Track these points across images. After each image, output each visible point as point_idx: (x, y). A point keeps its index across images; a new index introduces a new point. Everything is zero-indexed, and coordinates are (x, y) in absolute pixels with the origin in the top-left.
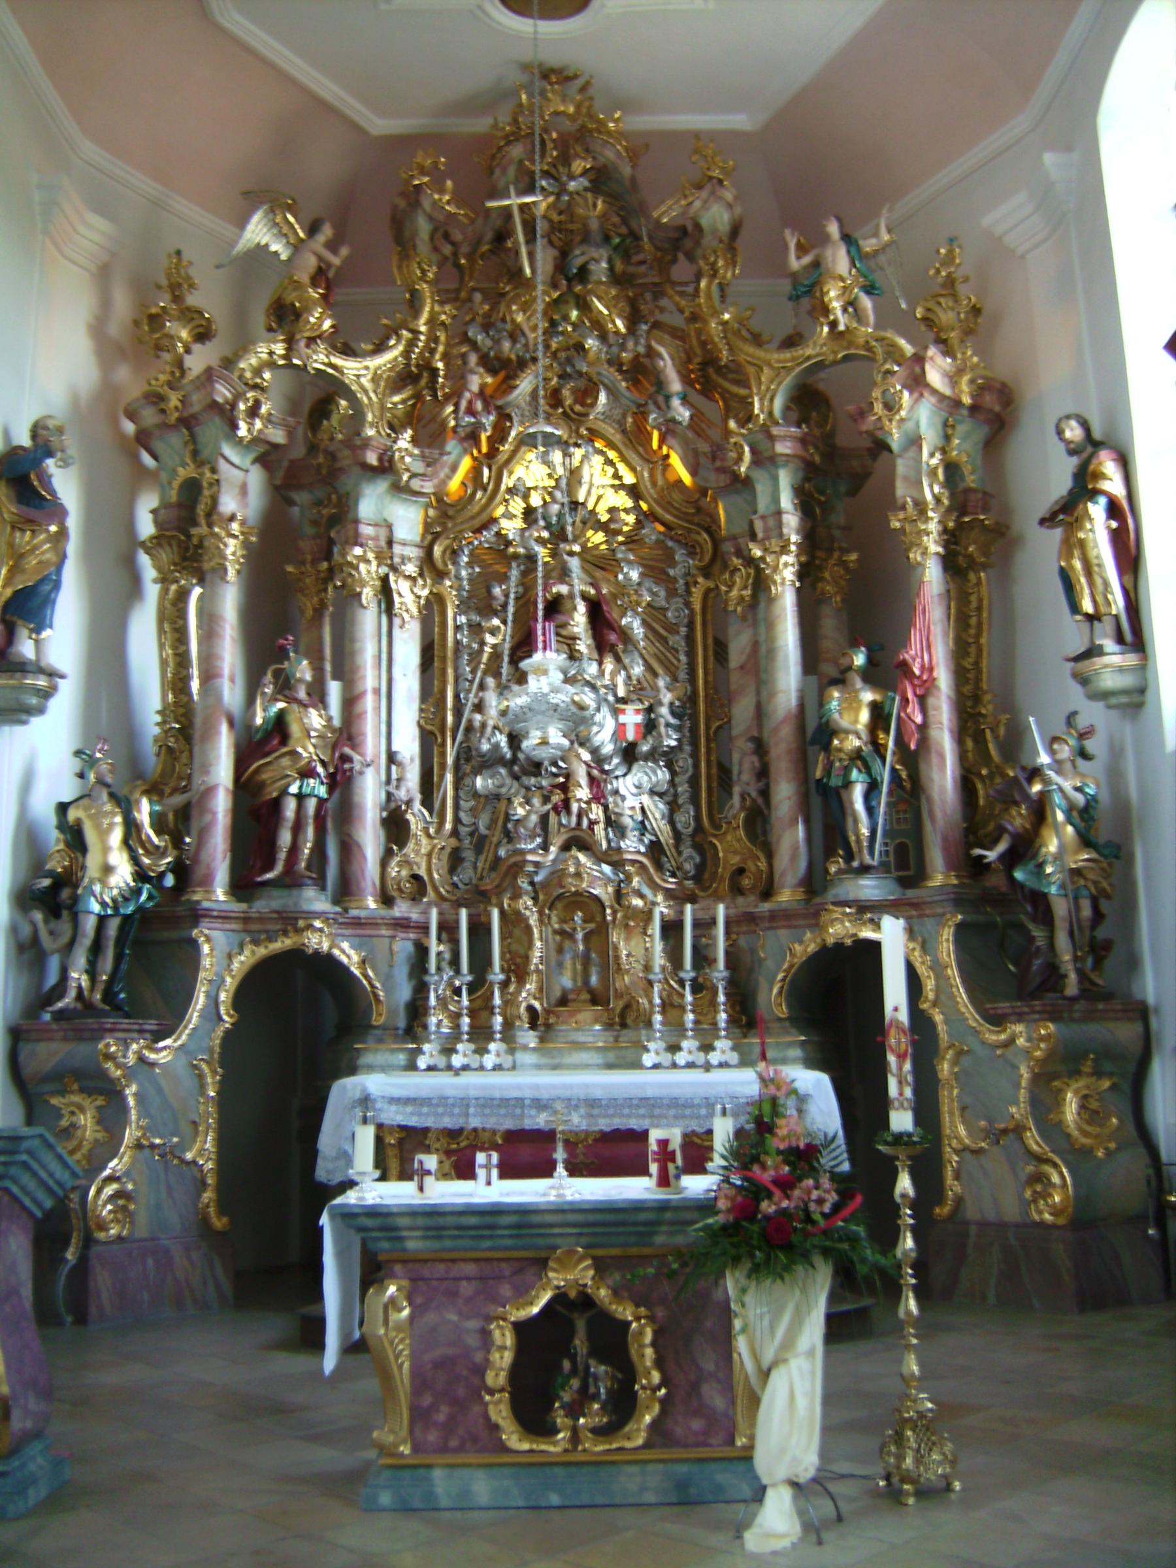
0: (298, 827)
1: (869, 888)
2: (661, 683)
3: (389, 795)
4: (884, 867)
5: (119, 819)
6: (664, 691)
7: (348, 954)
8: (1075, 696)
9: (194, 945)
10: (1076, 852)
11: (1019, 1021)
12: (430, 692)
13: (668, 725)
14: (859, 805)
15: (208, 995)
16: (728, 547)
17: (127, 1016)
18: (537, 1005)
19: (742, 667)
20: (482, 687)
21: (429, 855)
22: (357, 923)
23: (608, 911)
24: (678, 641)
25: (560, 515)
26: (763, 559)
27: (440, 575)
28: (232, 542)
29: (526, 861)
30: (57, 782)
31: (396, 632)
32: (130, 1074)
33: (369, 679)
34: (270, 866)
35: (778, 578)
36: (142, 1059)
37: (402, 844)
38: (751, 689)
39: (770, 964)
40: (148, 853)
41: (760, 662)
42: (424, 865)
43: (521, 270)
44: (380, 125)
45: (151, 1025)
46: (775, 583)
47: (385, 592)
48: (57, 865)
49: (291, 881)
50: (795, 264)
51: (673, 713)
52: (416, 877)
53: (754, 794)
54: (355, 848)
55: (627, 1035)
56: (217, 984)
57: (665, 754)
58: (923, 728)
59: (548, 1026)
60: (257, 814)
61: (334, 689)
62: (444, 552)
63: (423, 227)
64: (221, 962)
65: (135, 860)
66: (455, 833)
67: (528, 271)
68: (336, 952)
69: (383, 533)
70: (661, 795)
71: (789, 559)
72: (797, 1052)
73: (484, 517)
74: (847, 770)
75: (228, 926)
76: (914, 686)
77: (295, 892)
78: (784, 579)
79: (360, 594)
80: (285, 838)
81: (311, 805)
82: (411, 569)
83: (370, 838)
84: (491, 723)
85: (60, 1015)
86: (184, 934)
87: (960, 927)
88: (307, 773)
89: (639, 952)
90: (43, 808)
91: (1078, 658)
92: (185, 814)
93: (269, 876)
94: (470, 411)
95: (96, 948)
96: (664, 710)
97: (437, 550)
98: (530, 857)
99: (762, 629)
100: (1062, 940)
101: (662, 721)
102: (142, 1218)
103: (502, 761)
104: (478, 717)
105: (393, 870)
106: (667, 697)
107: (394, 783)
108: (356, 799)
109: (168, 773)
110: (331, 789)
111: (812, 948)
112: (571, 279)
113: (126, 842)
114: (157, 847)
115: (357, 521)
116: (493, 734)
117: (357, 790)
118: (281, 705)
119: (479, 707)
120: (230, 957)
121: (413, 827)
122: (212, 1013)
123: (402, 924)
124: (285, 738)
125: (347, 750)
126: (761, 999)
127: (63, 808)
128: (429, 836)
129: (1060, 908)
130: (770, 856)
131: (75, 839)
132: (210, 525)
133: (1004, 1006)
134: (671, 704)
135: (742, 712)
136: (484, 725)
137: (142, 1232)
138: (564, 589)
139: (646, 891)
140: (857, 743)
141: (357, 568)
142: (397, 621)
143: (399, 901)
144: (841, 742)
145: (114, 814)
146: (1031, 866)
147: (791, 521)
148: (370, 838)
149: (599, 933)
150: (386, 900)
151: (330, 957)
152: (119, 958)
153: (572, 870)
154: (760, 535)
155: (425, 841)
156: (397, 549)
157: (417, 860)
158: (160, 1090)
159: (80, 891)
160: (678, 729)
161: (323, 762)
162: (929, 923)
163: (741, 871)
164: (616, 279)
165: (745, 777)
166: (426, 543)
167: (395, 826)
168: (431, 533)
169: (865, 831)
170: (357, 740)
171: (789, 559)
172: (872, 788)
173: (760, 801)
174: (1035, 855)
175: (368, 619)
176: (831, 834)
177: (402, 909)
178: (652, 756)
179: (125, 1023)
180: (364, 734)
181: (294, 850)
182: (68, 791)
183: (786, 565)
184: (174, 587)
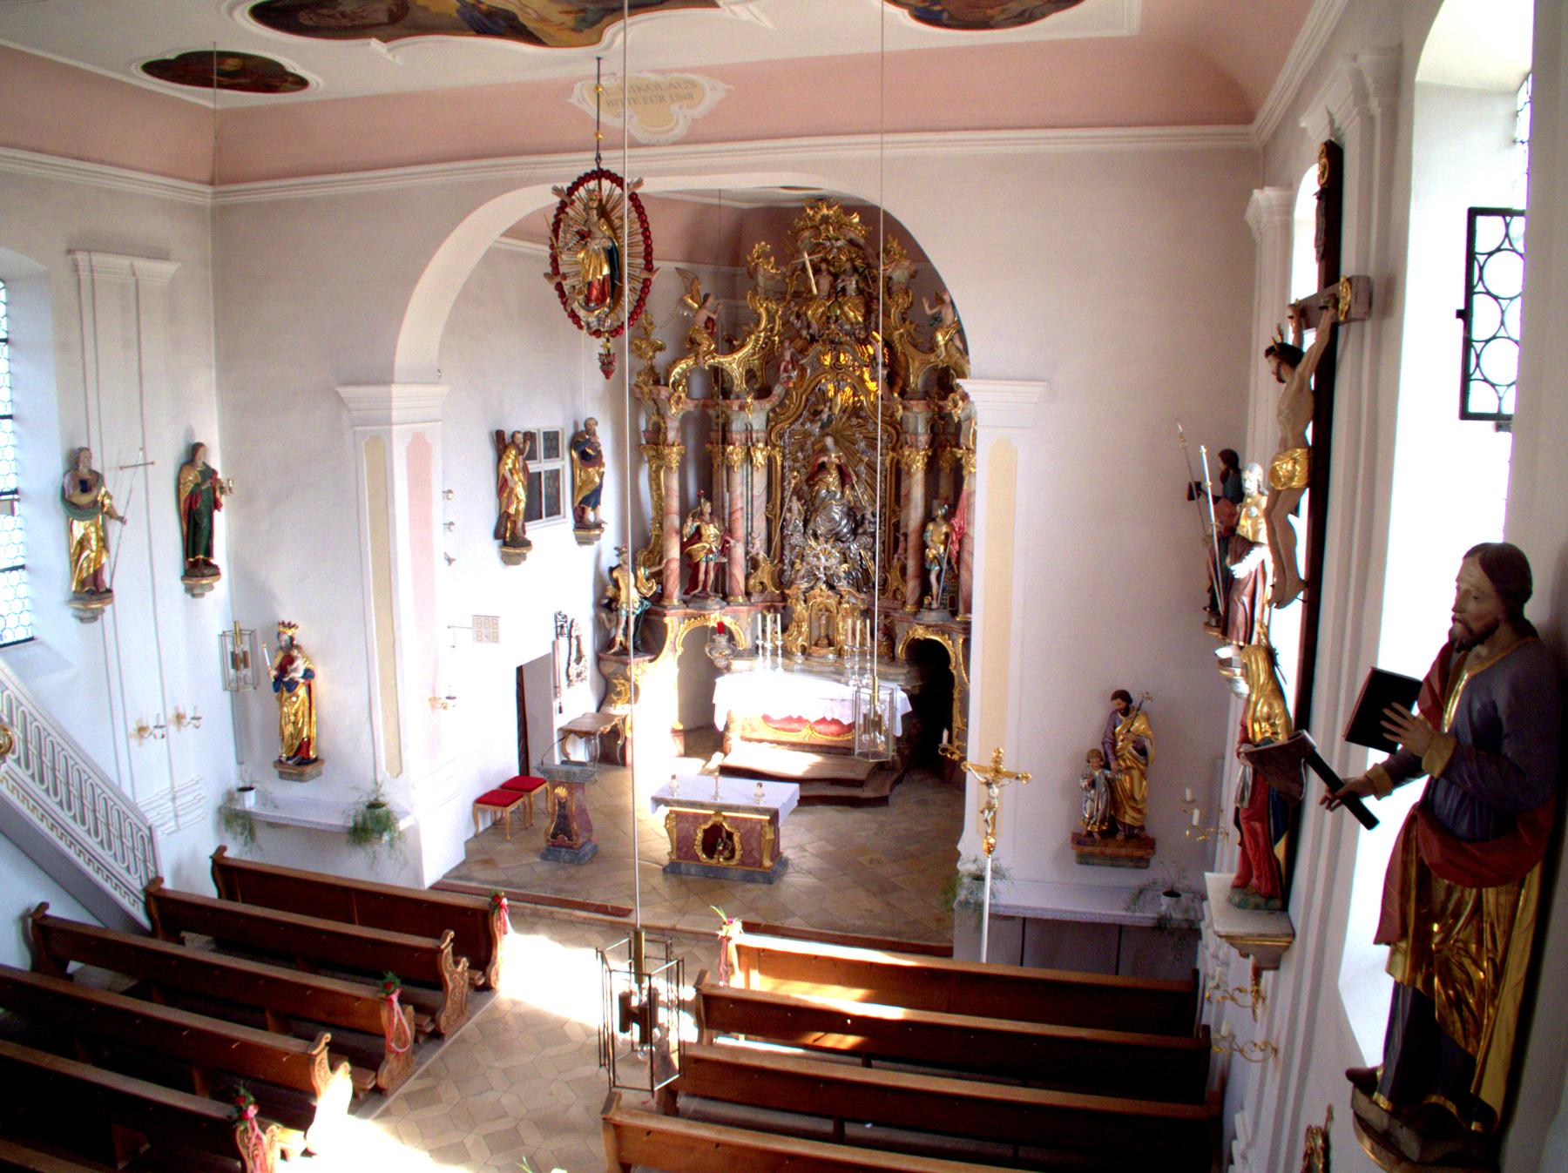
0: (706, 573)
43: (811, 291)
44: (746, 206)
48: (610, 592)
49: (704, 596)
50: (929, 312)
60: (690, 566)
63: (761, 280)
67: (815, 291)
80: (702, 576)
82: (761, 445)
83: (739, 572)
94: (786, 370)
105: (752, 582)
112: (837, 294)
119: (790, 510)
138: (825, 459)
148: (739, 572)
164: (860, 291)
167: (753, 564)
175: (738, 477)
176: (925, 588)
178: (865, 533)
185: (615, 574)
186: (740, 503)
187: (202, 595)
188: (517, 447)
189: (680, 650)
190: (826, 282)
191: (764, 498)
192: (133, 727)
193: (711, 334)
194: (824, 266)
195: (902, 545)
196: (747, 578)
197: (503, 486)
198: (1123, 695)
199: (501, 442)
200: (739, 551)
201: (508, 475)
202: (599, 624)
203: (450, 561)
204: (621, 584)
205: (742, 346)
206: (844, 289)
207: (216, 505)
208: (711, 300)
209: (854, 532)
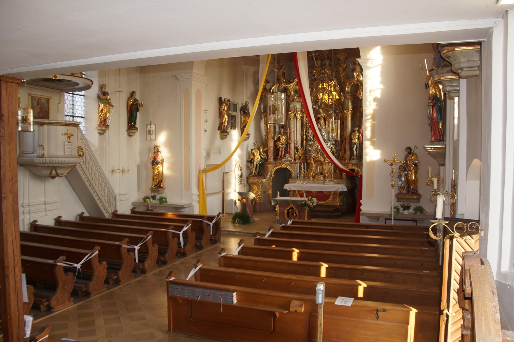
4: (358, 159)
7: (289, 167)
12: (302, 130)
27: (303, 113)
30: (251, 147)
32: (260, 183)
43: (315, 65)
47: (295, 116)
48: (251, 157)
50: (351, 67)
56: (272, 172)
60: (277, 150)
64: (271, 170)
65: (261, 157)
66: (306, 150)
80: (280, 153)
81: (284, 149)
88: (283, 144)
90: (250, 149)
105: (296, 156)
109: (265, 145)
119: (308, 133)
122: (271, 175)
124: (280, 140)
127: (252, 150)
131: (254, 154)
138: (320, 116)
151: (286, 168)
169: (355, 154)
172: (357, 147)
185: (253, 151)
186: (293, 130)
187: (132, 136)
188: (226, 103)
189: (273, 176)
190: (319, 62)
191: (300, 130)
192: (111, 170)
193: (284, 77)
194: (319, 57)
195: (344, 142)
196: (295, 155)
197: (221, 116)
198: (409, 148)
199: (221, 102)
200: (292, 145)
201: (223, 111)
202: (248, 167)
203: (205, 131)
204: (255, 154)
205: (293, 81)
206: (325, 64)
207: (138, 110)
208: (284, 67)
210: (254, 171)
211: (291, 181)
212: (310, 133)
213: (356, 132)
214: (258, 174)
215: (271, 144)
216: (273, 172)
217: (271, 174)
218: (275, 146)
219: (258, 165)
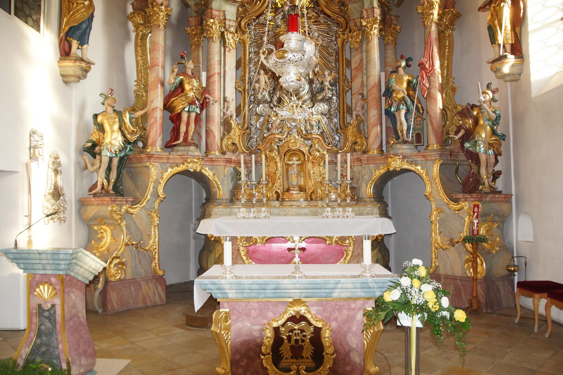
0: (188, 124)
1: (405, 149)
2: (326, 73)
3: (224, 114)
5: (117, 120)
6: (327, 76)
7: (208, 172)
8: (490, 77)
9: (148, 167)
10: (490, 137)
11: (466, 201)
13: (329, 89)
14: (403, 119)
15: (154, 188)
16: (352, 24)
17: (122, 195)
18: (279, 191)
19: (356, 68)
20: (259, 74)
21: (240, 135)
22: (212, 160)
23: (306, 157)
24: (332, 59)
25: (288, 11)
26: (366, 26)
28: (161, 14)
29: (275, 137)
31: (227, 53)
33: (216, 69)
34: (177, 139)
35: (372, 33)
36: (127, 211)
37: (229, 132)
38: (360, 76)
39: (366, 177)
40: (129, 133)
41: (363, 67)
42: (237, 140)
45: (130, 199)
46: (371, 34)
48: (95, 138)
51: (330, 84)
52: (234, 144)
53: (361, 115)
54: (211, 132)
55: (313, 203)
56: (157, 182)
57: (327, 100)
58: (429, 89)
59: (283, 200)
61: (204, 75)
62: (245, 24)
65: (124, 135)
68: (203, 171)
69: (221, 14)
70: (325, 115)
71: (376, 26)
72: (376, 210)
73: (260, 11)
74: (398, 106)
75: (161, 161)
76: (426, 73)
77: (187, 148)
78: (374, 34)
79: (212, 37)
80: (183, 128)
81: (193, 115)
82: (232, 29)
83: (216, 129)
84: (262, 87)
85: (95, 195)
86: (144, 164)
87: (441, 164)
88: (192, 103)
89: (317, 173)
91: (493, 62)
92: (145, 117)
93: (178, 142)
95: (109, 169)
96: (327, 84)
97: (243, 23)
98: (277, 136)
99: (364, 54)
100: (483, 171)
101: (327, 87)
102: (129, 271)
103: (266, 102)
104: (257, 85)
106: (329, 78)
107: (226, 109)
108: (211, 114)
110: (201, 110)
111: (382, 171)
113: (120, 128)
114: (133, 131)
115: (211, 9)
116: (263, 91)
117: (211, 111)
118: (181, 77)
119: (258, 81)
120: (162, 173)
121: (233, 126)
122: (156, 195)
123: (229, 161)
124: (183, 90)
125: (207, 95)
126: (363, 190)
127: (96, 116)
128: (239, 129)
129: (483, 158)
130: (367, 138)
131: (101, 128)
132: (153, 7)
133: (460, 196)
134: (330, 81)
135: (356, 85)
136: (260, 88)
137: (129, 276)
139: (320, 149)
140: (403, 95)
141: (211, 27)
142: (227, 49)
143: (228, 153)
144: (396, 94)
145: (116, 118)
146: (472, 142)
147: (377, 12)
148: (216, 129)
149: (302, 165)
150: (224, 153)
152: (119, 174)
153: (293, 141)
154: (365, 17)
155: (237, 130)
156: (227, 22)
157: (234, 137)
158: (135, 223)
159: (102, 148)
160: (332, 90)
161: (198, 99)
162: (429, 163)
163: (355, 143)
165: (358, 109)
166: (238, 20)
167: (226, 125)
168: (240, 17)
169: (405, 128)
170: (211, 92)
171: (376, 26)
172: (408, 111)
173: (363, 117)
174: (474, 138)
175: (216, 46)
177: (229, 155)
178: (322, 100)
179: (120, 198)
180: (214, 90)
181: (187, 133)
182: (100, 109)
183: (375, 28)
184: (141, 33)
185: (99, 119)
196: (222, 139)
200: (216, 111)
204: (107, 127)
209: (314, 100)
210: (100, 178)
211: (216, 210)
212: (263, 83)
213: (401, 71)
214: (115, 188)
215: (157, 100)
216: (163, 183)
217: (155, 188)
218: (168, 107)
219: (116, 161)
